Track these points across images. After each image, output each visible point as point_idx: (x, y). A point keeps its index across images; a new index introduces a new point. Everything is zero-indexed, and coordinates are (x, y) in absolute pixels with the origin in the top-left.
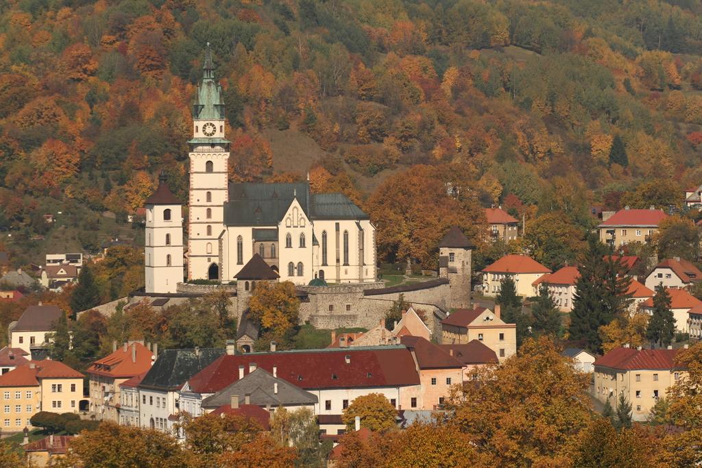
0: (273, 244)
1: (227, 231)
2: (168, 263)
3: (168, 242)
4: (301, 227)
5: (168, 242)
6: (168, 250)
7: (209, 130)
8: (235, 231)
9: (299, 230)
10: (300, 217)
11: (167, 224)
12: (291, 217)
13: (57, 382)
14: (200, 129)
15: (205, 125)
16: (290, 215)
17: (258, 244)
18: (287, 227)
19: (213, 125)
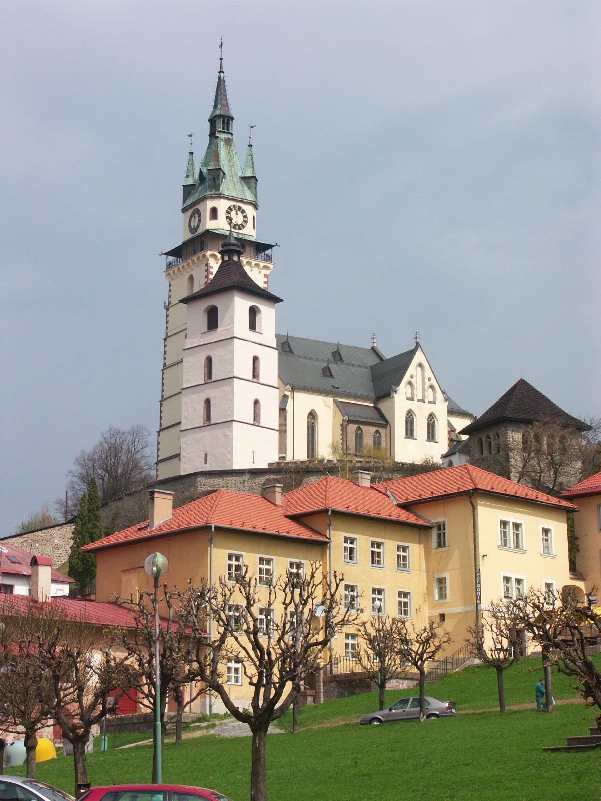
0: (377, 431)
1: (290, 401)
2: (255, 419)
3: (255, 375)
4: (430, 402)
5: (255, 375)
6: (257, 392)
7: (238, 219)
8: (303, 402)
9: (427, 408)
10: (427, 384)
11: (252, 336)
12: (413, 381)
13: (513, 516)
14: (222, 214)
15: (230, 208)
16: (412, 377)
17: (352, 428)
18: (408, 399)
19: (243, 212)
